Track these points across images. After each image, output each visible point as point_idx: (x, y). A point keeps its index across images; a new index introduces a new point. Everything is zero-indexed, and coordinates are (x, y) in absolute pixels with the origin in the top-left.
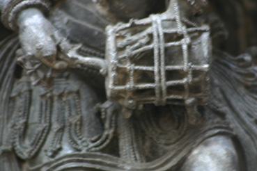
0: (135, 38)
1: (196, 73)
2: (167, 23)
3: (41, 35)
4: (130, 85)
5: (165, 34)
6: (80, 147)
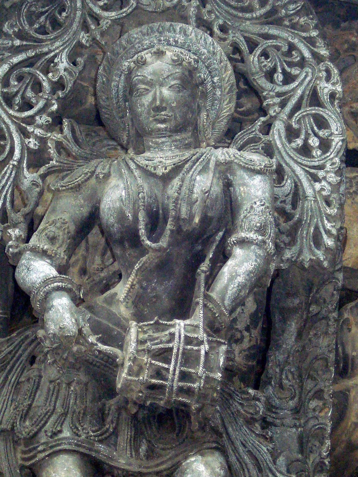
0: (156, 335)
1: (208, 379)
2: (189, 328)
3: (67, 315)
4: (144, 376)
5: (186, 337)
6: (81, 432)
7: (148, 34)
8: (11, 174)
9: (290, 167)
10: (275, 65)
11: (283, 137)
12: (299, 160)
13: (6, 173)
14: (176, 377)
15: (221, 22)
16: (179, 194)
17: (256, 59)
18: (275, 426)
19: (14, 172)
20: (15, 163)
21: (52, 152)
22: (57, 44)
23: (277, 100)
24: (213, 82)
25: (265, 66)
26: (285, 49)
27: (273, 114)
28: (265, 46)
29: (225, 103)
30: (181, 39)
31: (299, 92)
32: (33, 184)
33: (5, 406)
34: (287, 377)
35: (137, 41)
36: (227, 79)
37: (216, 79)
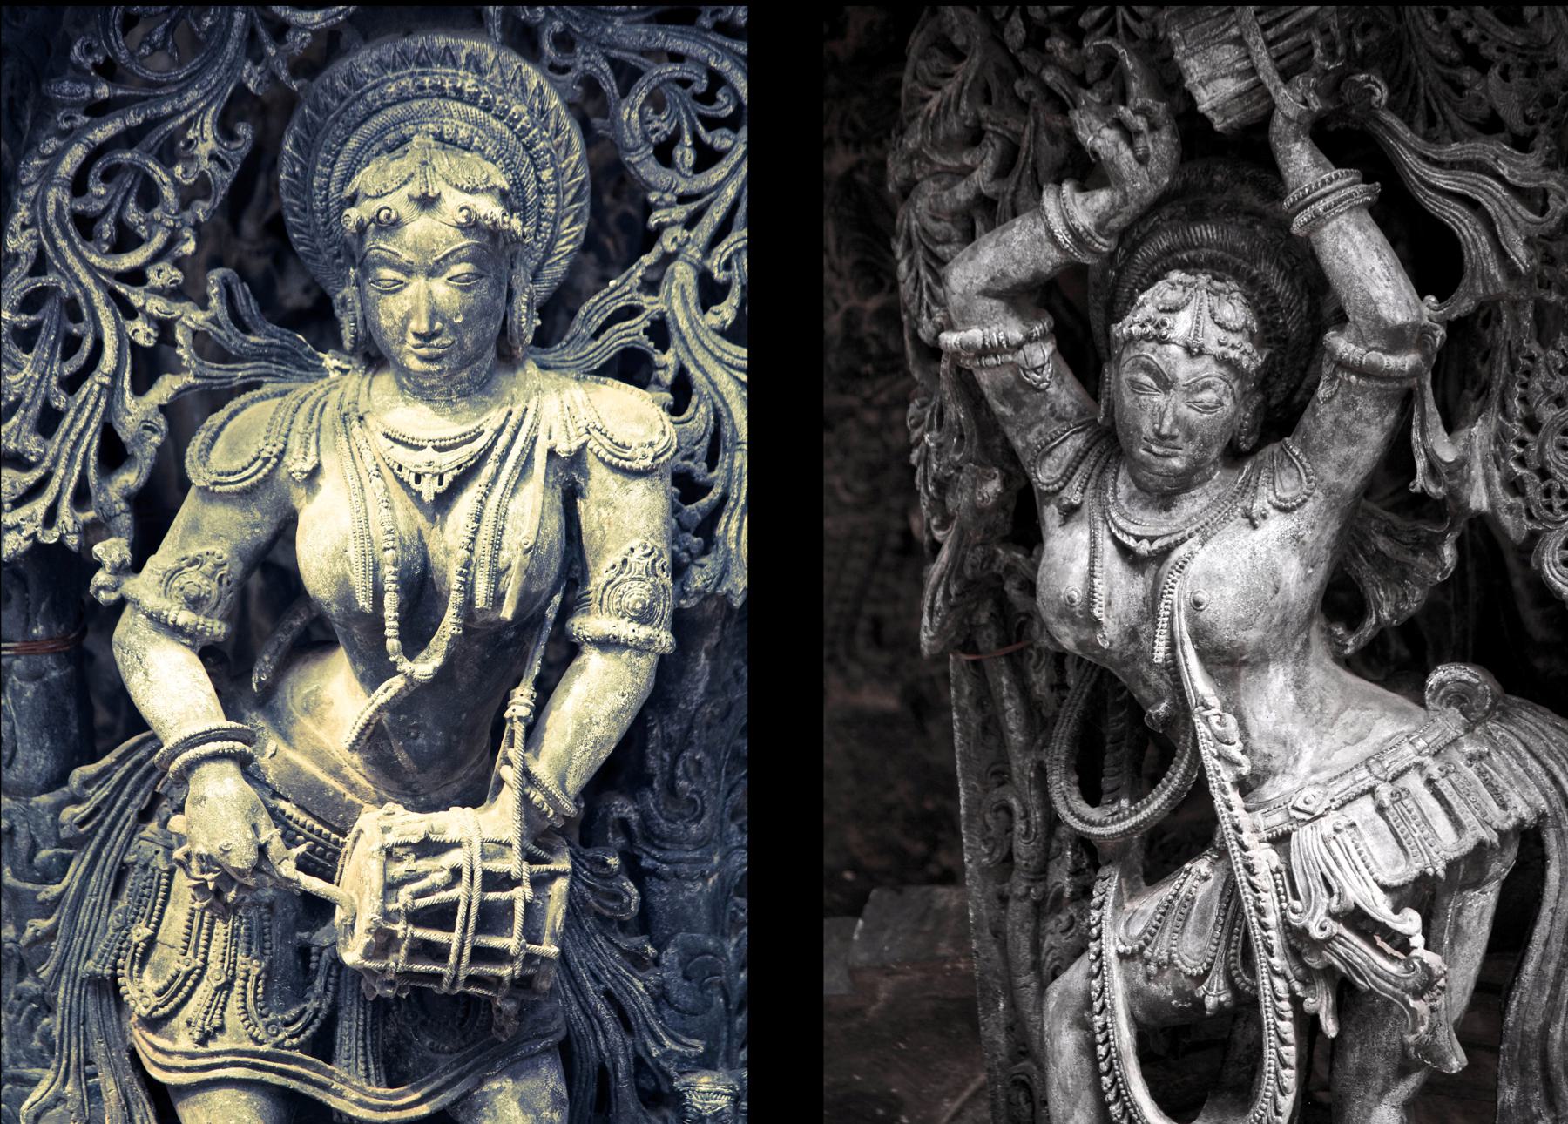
0: (423, 865)
1: (530, 958)
2: (492, 848)
4: (397, 961)
7: (395, 69)
8: (96, 404)
9: (705, 373)
10: (679, 127)
11: (692, 304)
12: (726, 357)
13: (85, 401)
14: (465, 960)
15: (558, 26)
16: (471, 551)
17: (635, 116)
18: (660, 877)
19: (103, 400)
20: (106, 380)
21: (186, 357)
22: (192, 95)
23: (680, 212)
24: (539, 180)
25: (656, 130)
26: (701, 85)
27: (672, 248)
28: (655, 82)
29: (567, 222)
30: (469, 83)
31: (730, 192)
32: (146, 428)
33: (95, 918)
34: (686, 772)
35: (370, 83)
36: (570, 172)
37: (546, 175)
